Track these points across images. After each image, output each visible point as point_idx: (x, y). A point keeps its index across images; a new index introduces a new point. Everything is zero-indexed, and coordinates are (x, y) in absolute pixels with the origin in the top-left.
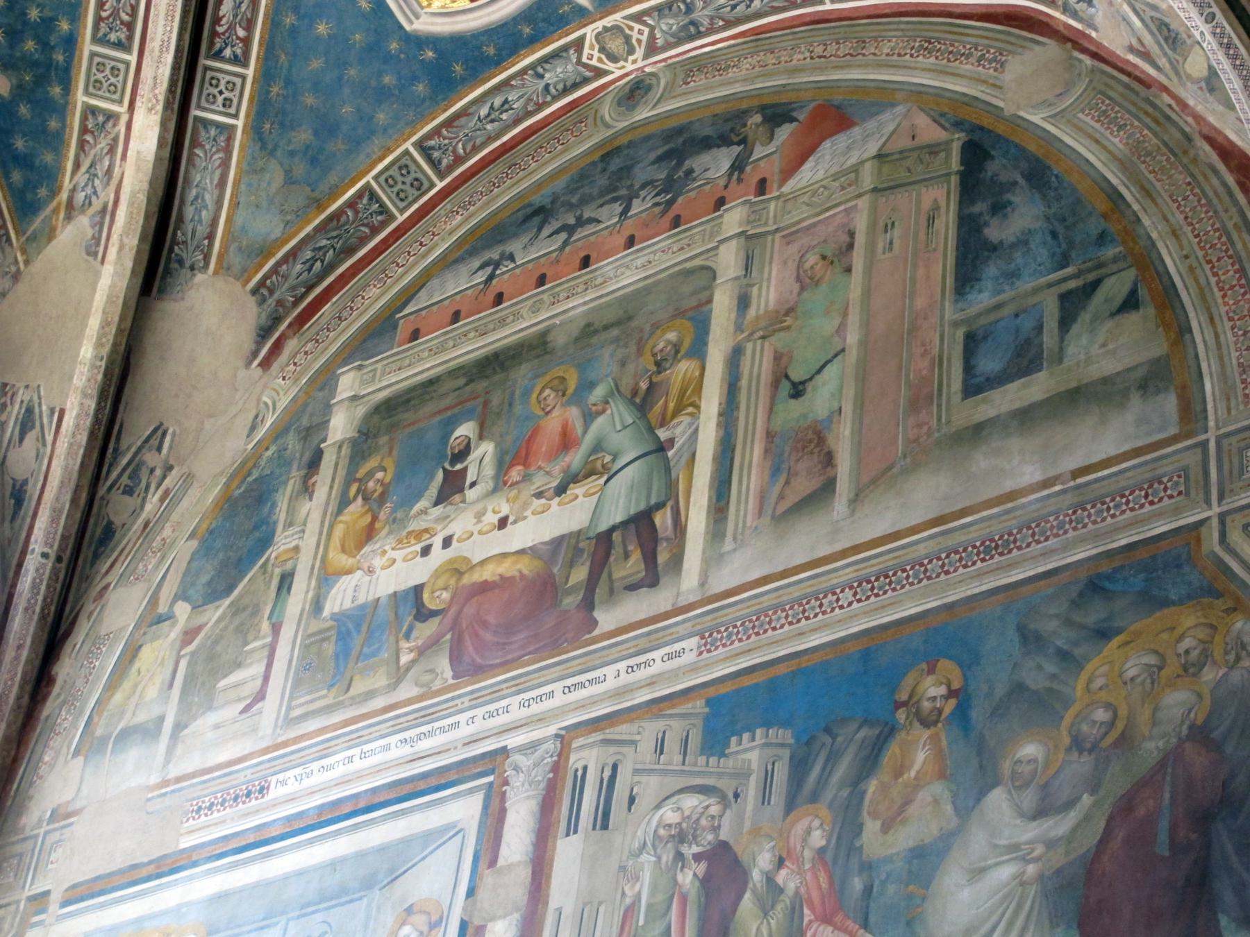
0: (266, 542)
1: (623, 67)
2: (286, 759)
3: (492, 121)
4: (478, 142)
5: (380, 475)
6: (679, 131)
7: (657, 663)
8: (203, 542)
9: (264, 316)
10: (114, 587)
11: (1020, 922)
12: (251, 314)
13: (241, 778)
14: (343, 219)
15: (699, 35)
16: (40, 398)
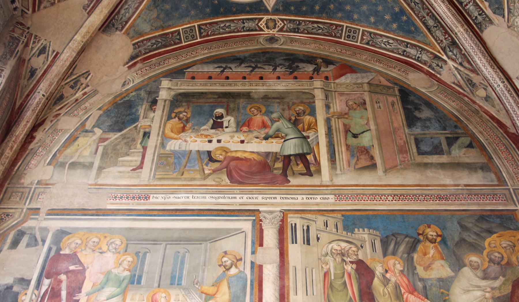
0: (135, 120)
1: (269, 31)
2: (156, 190)
3: (223, 29)
4: (216, 33)
5: (185, 114)
6: (292, 55)
7: (318, 199)
8: (105, 112)
9: (134, 53)
10: (63, 115)
12: (130, 51)
13: (135, 191)
14: (168, 36)
15: (298, 32)
16: (50, 45)
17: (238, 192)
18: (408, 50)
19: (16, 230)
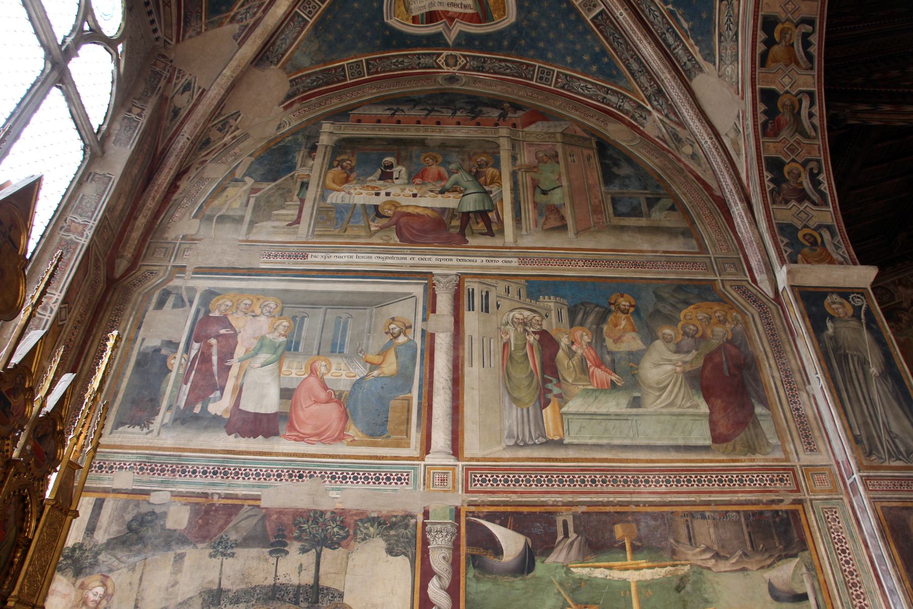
0: (292, 168)
4: (387, 69)
5: (349, 162)
6: (475, 97)
7: (500, 262)
8: (257, 159)
11: (678, 384)
12: (286, 88)
13: (291, 249)
15: (482, 72)
17: (409, 252)
18: (609, 97)
19: (161, 289)
